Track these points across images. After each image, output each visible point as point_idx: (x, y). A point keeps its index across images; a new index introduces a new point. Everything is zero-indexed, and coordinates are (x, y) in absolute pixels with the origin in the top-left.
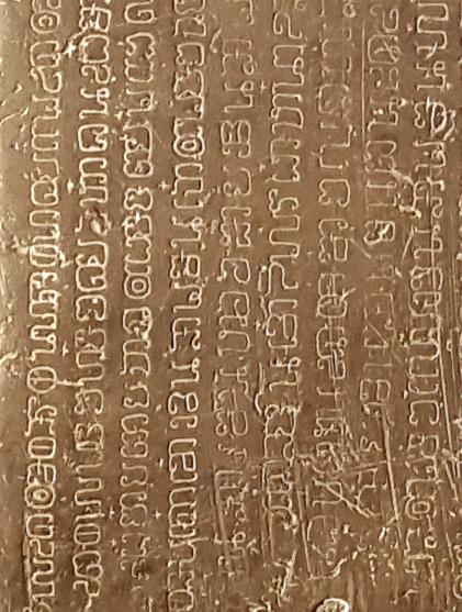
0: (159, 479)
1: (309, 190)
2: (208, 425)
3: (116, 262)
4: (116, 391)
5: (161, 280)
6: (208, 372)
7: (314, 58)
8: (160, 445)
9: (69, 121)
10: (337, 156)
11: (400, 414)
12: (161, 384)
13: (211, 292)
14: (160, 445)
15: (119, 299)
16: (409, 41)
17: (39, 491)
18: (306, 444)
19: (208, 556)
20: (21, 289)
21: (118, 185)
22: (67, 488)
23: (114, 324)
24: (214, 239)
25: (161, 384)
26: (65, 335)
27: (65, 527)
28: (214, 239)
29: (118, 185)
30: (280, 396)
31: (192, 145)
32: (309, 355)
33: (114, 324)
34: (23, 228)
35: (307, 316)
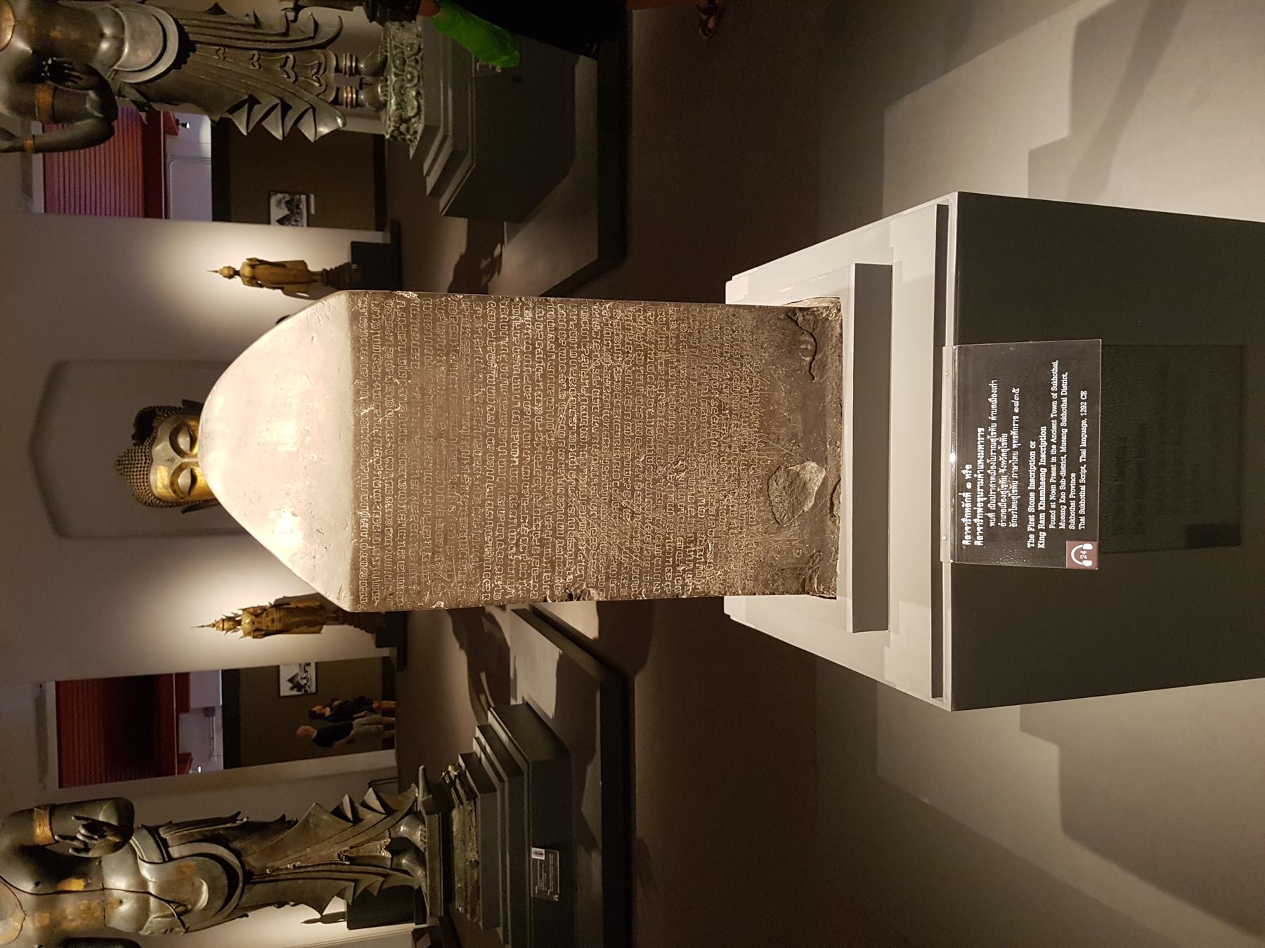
0: (394, 572)
1: (433, 498)
2: (407, 557)
3: (383, 516)
4: (383, 549)
5: (395, 521)
6: (407, 544)
7: (434, 464)
8: (394, 563)
9: (371, 480)
10: (440, 489)
11: (457, 555)
12: (395, 549)
13: (408, 524)
14: (394, 563)
15: (384, 526)
16: (459, 460)
17: (363, 574)
18: (433, 562)
19: (407, 591)
20: (358, 523)
21: (383, 497)
22: (370, 573)
23: (383, 532)
24: (409, 510)
25: (395, 549)
26: (370, 535)
27: (369, 584)
28: (409, 510)
29: (383, 497)
30: (426, 550)
31: (403, 486)
32: (433, 540)
33: (383, 532)
34: (358, 507)
35: (433, 530)
